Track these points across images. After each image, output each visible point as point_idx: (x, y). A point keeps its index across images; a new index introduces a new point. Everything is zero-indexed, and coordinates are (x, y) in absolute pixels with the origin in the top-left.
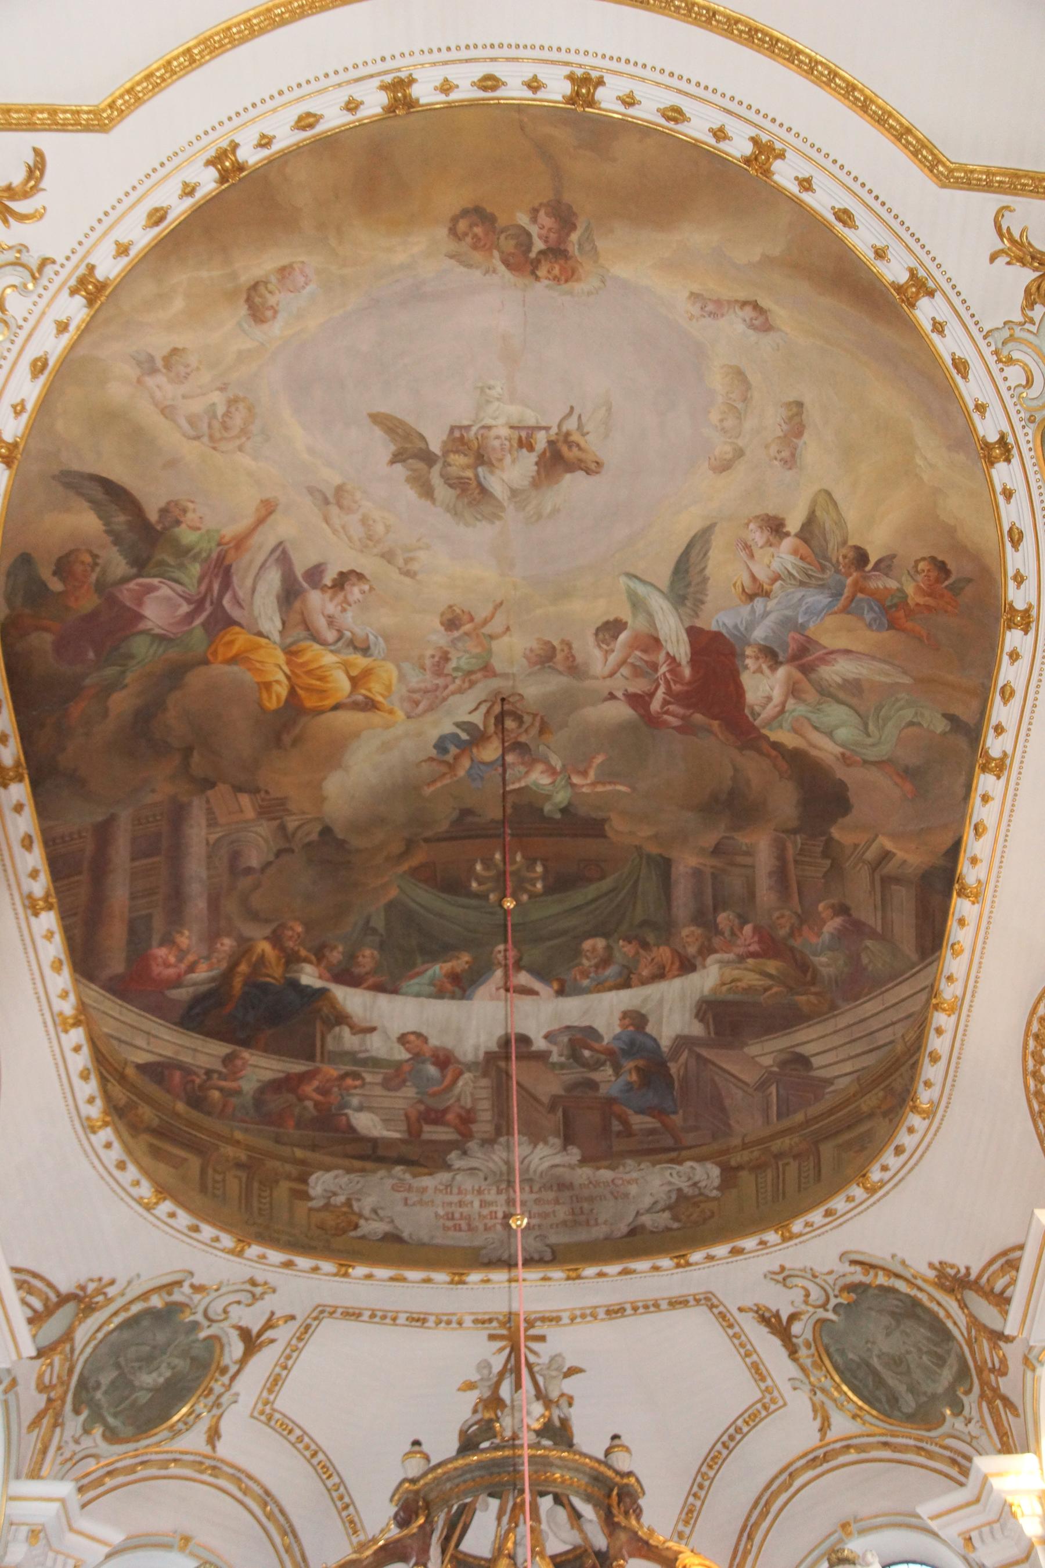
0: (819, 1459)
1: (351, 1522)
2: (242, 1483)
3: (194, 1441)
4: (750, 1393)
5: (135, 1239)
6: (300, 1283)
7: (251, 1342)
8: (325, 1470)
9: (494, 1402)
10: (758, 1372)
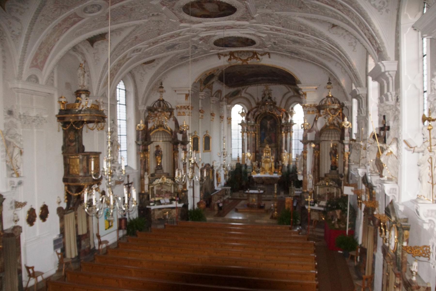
0: (294, 96)
2: (244, 98)
3: (240, 95)
4: (288, 91)
5: (232, 90)
6: (247, 86)
7: (243, 89)
8: (251, 95)
9: (265, 94)
10: (289, 90)
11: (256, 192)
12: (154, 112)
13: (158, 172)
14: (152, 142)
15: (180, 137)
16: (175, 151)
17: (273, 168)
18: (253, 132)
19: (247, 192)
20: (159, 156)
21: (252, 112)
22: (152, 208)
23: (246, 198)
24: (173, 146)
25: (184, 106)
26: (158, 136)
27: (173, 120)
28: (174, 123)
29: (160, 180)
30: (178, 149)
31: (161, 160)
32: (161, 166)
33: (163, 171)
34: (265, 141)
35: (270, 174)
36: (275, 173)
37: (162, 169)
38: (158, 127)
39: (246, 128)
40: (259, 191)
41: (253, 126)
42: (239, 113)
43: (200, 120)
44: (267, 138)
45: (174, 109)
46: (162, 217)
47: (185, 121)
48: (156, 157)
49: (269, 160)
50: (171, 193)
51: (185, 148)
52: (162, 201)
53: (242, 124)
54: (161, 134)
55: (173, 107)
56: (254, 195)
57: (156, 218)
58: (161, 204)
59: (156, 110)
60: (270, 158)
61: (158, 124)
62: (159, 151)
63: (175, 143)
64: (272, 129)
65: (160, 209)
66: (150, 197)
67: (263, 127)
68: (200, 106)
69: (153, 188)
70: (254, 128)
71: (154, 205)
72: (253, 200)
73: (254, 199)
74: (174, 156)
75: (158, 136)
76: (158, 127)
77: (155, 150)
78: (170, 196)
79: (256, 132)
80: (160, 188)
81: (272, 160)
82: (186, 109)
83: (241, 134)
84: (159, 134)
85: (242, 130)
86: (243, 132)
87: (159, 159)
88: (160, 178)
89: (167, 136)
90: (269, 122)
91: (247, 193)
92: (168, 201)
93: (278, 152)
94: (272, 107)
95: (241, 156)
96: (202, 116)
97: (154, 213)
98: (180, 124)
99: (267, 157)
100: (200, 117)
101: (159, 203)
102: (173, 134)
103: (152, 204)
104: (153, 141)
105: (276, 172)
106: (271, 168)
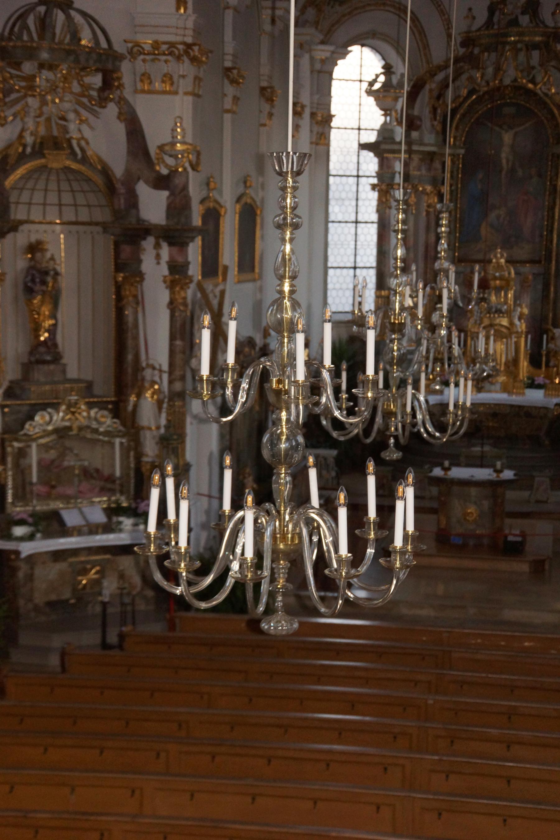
1: (442, 11)
11: (483, 474)
12: (17, 65)
13: (40, 374)
14: (15, 227)
15: (153, 206)
16: (126, 270)
17: (524, 364)
18: (429, 188)
19: (437, 472)
20: (44, 293)
21: (431, 86)
22: (27, 549)
23: (435, 505)
24: (117, 245)
25: (172, 45)
26: (38, 197)
27: (120, 116)
28: (120, 129)
29: (59, 417)
30: (140, 261)
31: (53, 316)
32: (55, 345)
33: (64, 372)
34: (484, 230)
35: (505, 389)
36: (532, 385)
37: (57, 358)
38: (39, 150)
39: (399, 167)
40: (498, 472)
41: (430, 157)
42: (369, 92)
43: (227, 117)
44: (492, 216)
45: (121, 58)
46: (67, 594)
47: (169, 118)
48: (29, 301)
49: (505, 322)
50: (110, 479)
51: (180, 259)
52: (71, 518)
53: (381, 147)
54: (53, 185)
55: (119, 47)
56: (473, 491)
57: (39, 599)
58: (64, 531)
59: (31, 53)
60: (509, 314)
61: (42, 130)
62: (46, 273)
63: (129, 235)
64: (520, 173)
65: (58, 556)
66: (10, 499)
67: (476, 162)
68: (229, 47)
69: (22, 453)
70: (437, 165)
71: (31, 537)
72: (466, 514)
73: (472, 509)
74: (119, 298)
75: (38, 197)
76: (39, 150)
77: (22, 264)
78: (103, 491)
79: (446, 189)
80: (52, 454)
81: (521, 326)
82: (179, 58)
83: (375, 195)
84: (41, 185)
85: (379, 175)
86: (384, 185)
87: (46, 310)
88: (56, 406)
89: (81, 200)
90: (507, 138)
91: (438, 481)
92: (97, 516)
93: (546, 287)
94: (536, 54)
95: (369, 304)
96: (236, 99)
97: (30, 577)
98: (154, 138)
99: (499, 311)
100: (228, 103)
101: (50, 524)
102: (116, 192)
103: (19, 531)
104: (22, 222)
105: (540, 380)
106: (515, 361)
